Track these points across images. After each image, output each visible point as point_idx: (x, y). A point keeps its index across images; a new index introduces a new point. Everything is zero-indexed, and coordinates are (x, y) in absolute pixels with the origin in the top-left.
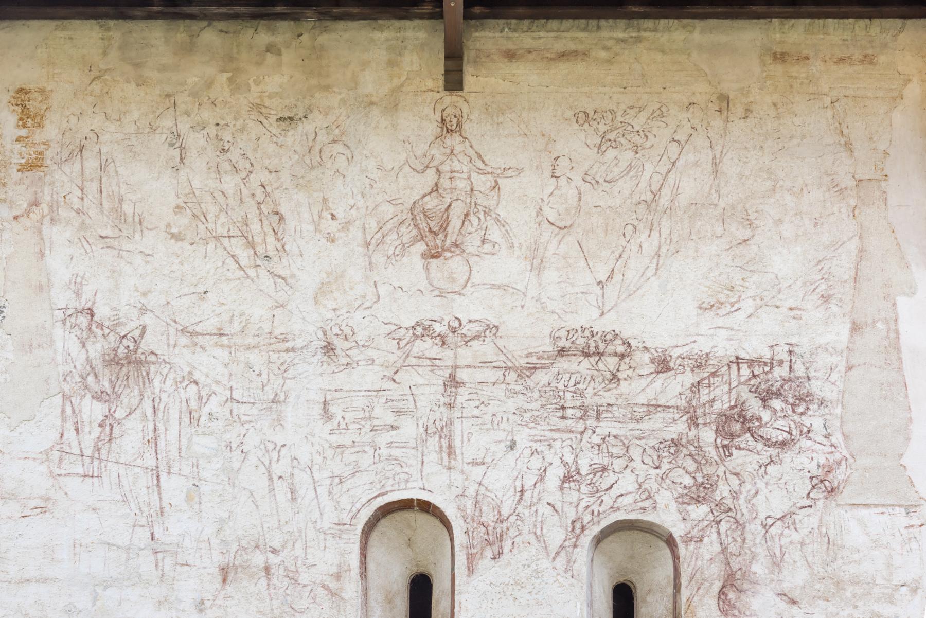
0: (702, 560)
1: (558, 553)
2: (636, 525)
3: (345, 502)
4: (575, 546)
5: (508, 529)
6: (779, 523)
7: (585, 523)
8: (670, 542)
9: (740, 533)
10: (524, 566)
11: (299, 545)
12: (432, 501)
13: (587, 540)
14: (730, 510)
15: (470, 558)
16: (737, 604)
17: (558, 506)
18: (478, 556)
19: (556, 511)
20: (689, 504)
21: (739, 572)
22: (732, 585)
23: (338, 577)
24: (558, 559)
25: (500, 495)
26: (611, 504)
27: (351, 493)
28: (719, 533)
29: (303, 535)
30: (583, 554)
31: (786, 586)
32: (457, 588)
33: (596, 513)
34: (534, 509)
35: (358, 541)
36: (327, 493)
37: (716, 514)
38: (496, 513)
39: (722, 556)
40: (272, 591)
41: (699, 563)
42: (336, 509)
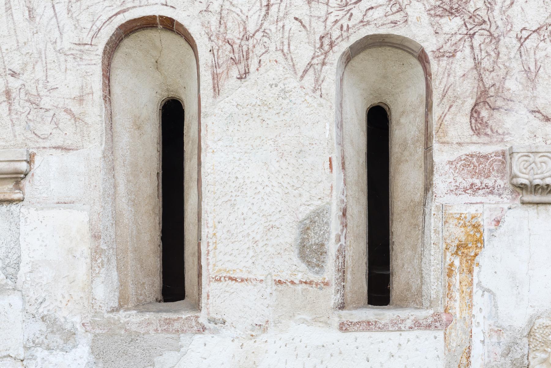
0: (454, 77)
1: (306, 71)
2: (387, 40)
3: (85, 19)
4: (324, 64)
5: (254, 47)
6: (535, 35)
7: (334, 38)
8: (422, 58)
9: (494, 47)
10: (271, 86)
11: (39, 67)
12: (175, 18)
13: (335, 57)
14: (484, 22)
15: (215, 77)
16: (490, 123)
17: (306, 21)
18: (224, 76)
19: (304, 26)
20: (441, 16)
21: (492, 89)
22: (485, 102)
23: (81, 100)
24: (306, 78)
25: (245, 9)
26: (361, 18)
27: (91, 10)
28: (472, 47)
29: (43, 56)
30: (331, 73)
31: (540, 103)
32: (203, 110)
33: (345, 28)
34: (280, 24)
35: (100, 61)
36: (66, 11)
37: (469, 27)
38: (241, 29)
39: (475, 72)
40: (14, 116)
41: (452, 79)
42: (76, 28)
